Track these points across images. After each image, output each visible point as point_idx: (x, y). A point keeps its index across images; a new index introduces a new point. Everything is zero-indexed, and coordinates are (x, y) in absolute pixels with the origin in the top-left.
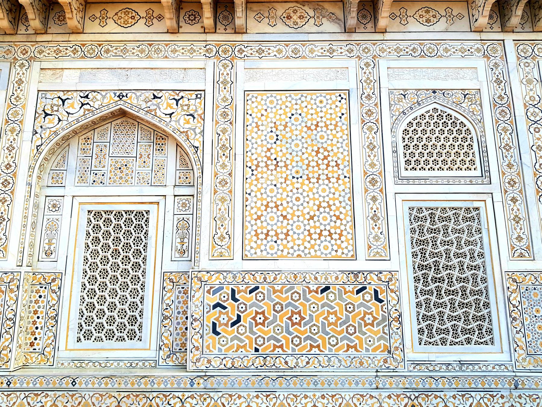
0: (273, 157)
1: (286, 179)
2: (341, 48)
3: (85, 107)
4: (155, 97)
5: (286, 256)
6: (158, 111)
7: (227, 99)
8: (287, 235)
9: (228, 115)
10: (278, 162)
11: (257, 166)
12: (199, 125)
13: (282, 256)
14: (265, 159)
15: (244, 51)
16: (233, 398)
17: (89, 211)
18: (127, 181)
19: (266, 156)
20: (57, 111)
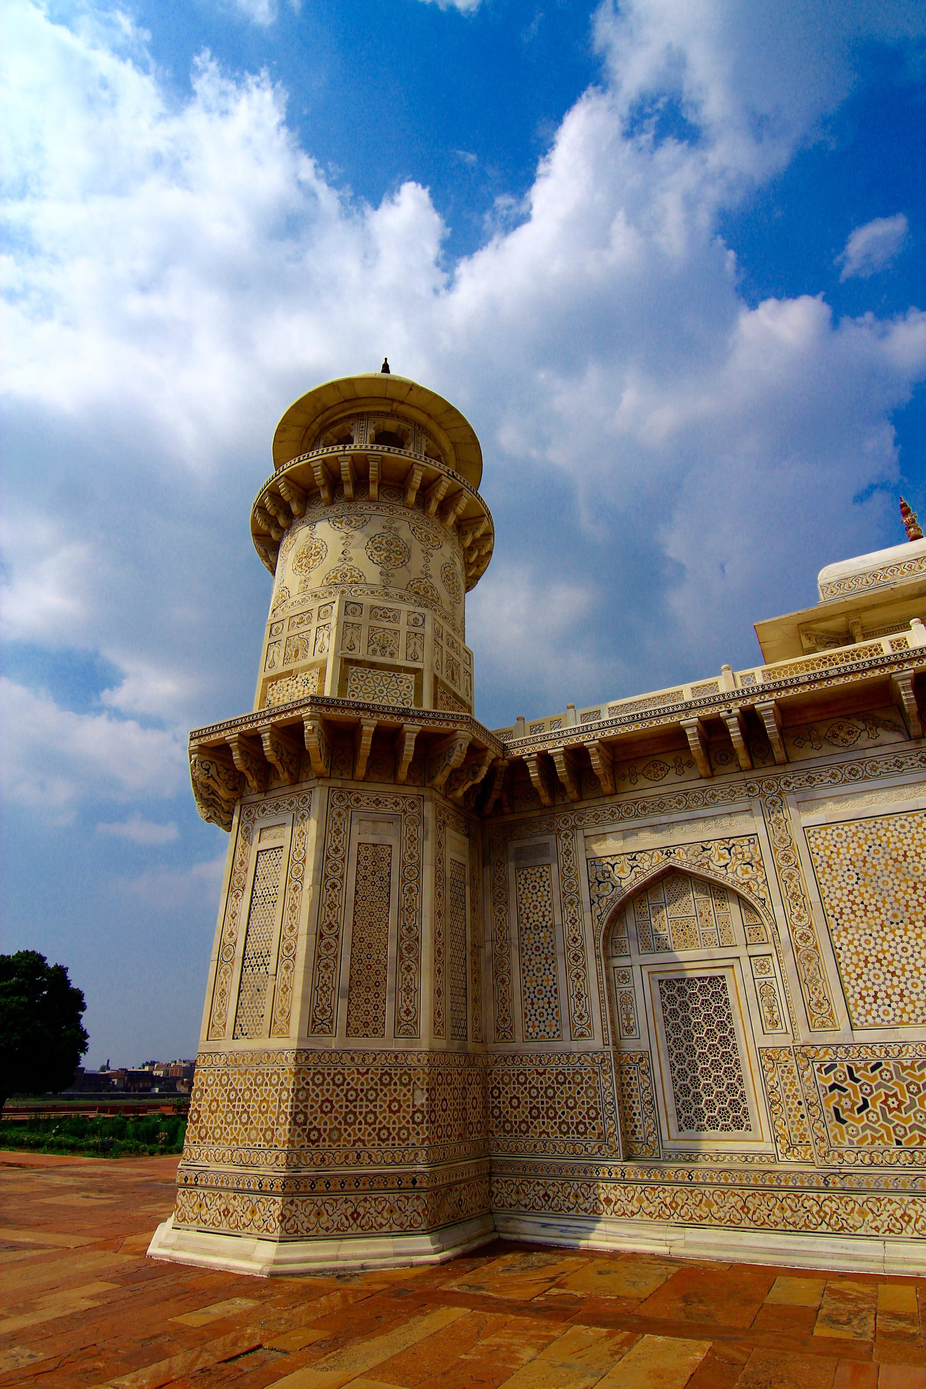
0: (858, 900)
1: (882, 926)
2: (911, 759)
3: (635, 869)
4: (704, 849)
5: (907, 1023)
6: (710, 863)
7: (785, 840)
8: (901, 995)
9: (790, 858)
10: (866, 906)
11: (841, 913)
12: (760, 873)
13: (901, 1023)
14: (849, 904)
15: (791, 783)
16: (883, 1202)
17: (660, 981)
18: (692, 944)
19: (849, 900)
20: (609, 877)
